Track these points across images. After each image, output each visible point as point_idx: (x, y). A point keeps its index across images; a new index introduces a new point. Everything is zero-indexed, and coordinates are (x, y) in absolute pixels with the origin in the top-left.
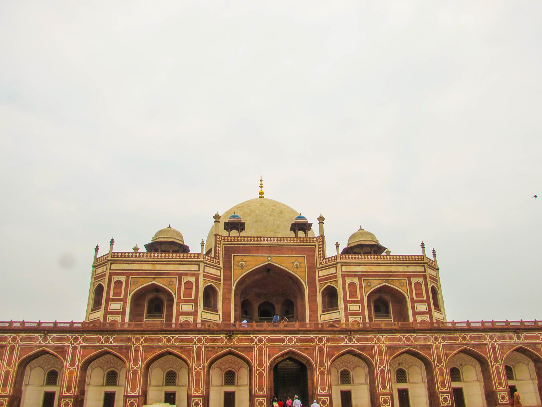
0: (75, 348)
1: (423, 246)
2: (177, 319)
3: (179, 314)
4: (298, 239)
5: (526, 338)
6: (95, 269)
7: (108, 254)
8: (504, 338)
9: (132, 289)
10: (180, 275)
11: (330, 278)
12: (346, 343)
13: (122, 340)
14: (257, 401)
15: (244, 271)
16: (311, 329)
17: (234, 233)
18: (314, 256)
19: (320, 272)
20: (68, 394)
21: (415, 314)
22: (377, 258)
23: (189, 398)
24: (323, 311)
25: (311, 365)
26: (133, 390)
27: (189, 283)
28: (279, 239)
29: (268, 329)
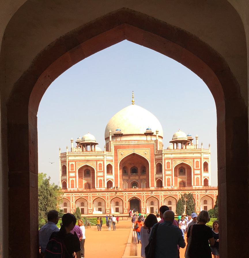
0: (72, 197)
1: (202, 144)
2: (97, 179)
3: (97, 177)
4: (147, 141)
5: (209, 192)
6: (60, 158)
7: (66, 153)
8: (202, 192)
10: (97, 161)
11: (159, 160)
13: (85, 195)
16: (141, 190)
19: (156, 156)
20: (73, 209)
21: (194, 175)
25: (140, 201)
26: (90, 208)
27: (100, 164)
28: (138, 141)
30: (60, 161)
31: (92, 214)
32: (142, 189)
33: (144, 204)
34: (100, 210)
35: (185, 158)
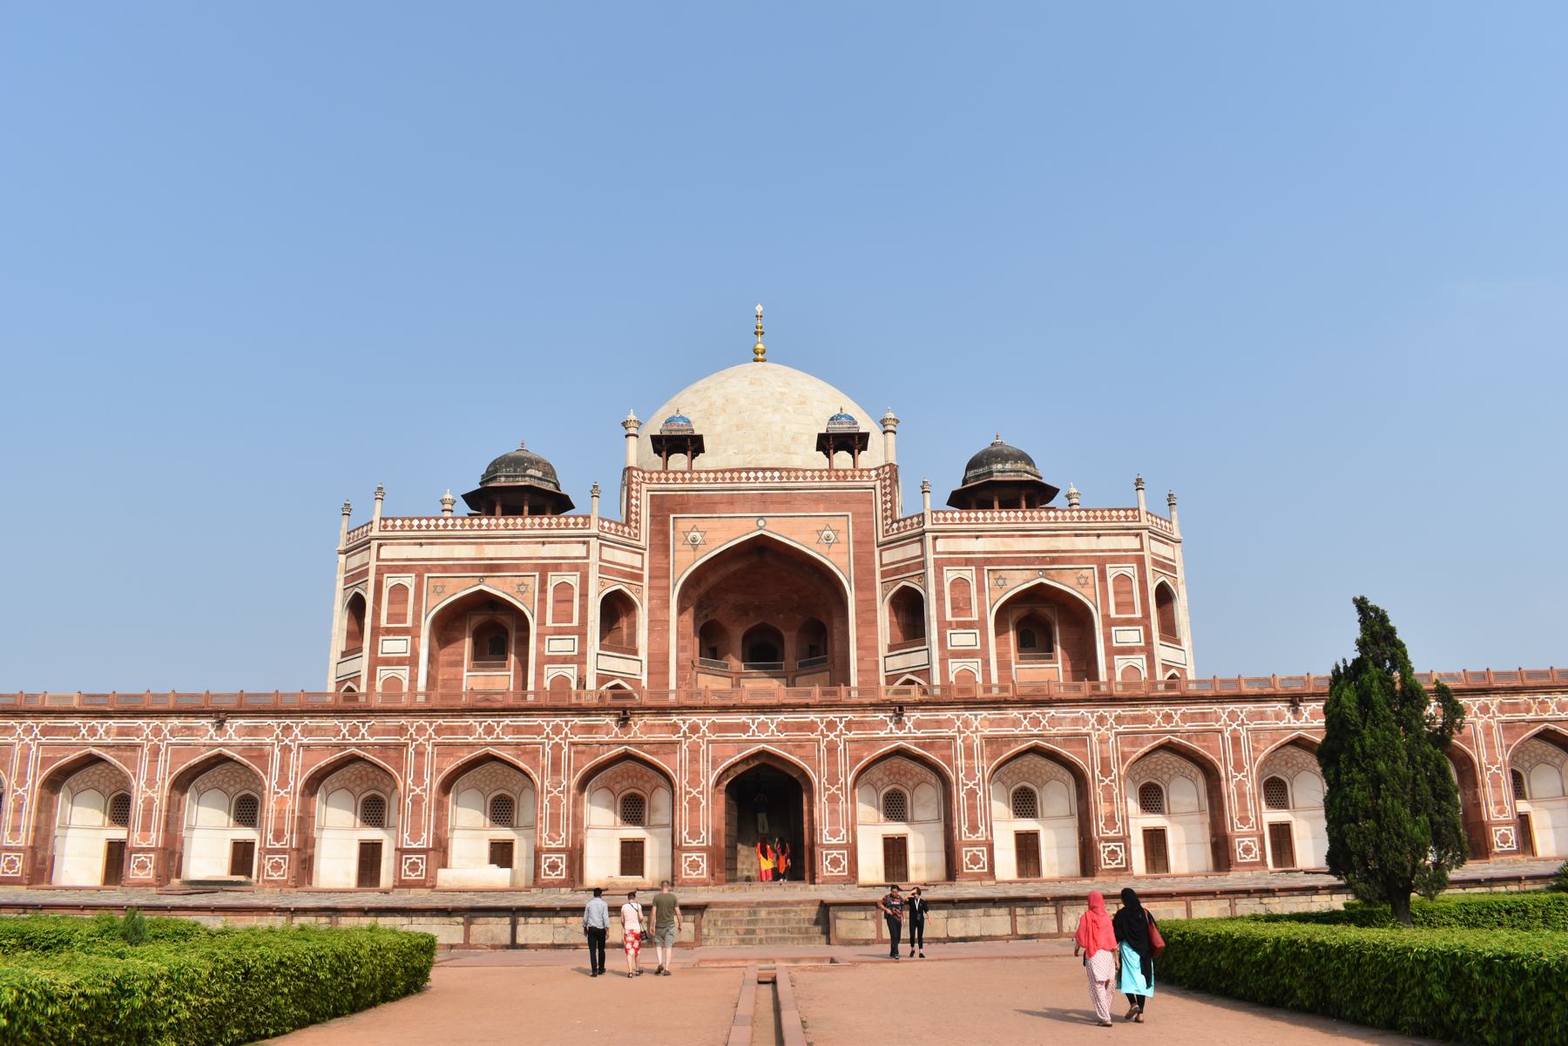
0: (286, 750)
6: (342, 558)
8: (1262, 716)
9: (431, 605)
10: (544, 570)
11: (908, 568)
12: (890, 733)
13: (387, 732)
14: (686, 859)
15: (699, 554)
16: (810, 701)
17: (679, 461)
18: (869, 514)
21: (1112, 652)
22: (1024, 518)
23: (538, 853)
24: (891, 648)
26: (415, 836)
27: (564, 588)
28: (785, 474)
29: (712, 703)
30: (341, 577)
31: (428, 883)
32: (824, 694)
33: (841, 807)
34: (501, 854)
35: (1053, 561)
